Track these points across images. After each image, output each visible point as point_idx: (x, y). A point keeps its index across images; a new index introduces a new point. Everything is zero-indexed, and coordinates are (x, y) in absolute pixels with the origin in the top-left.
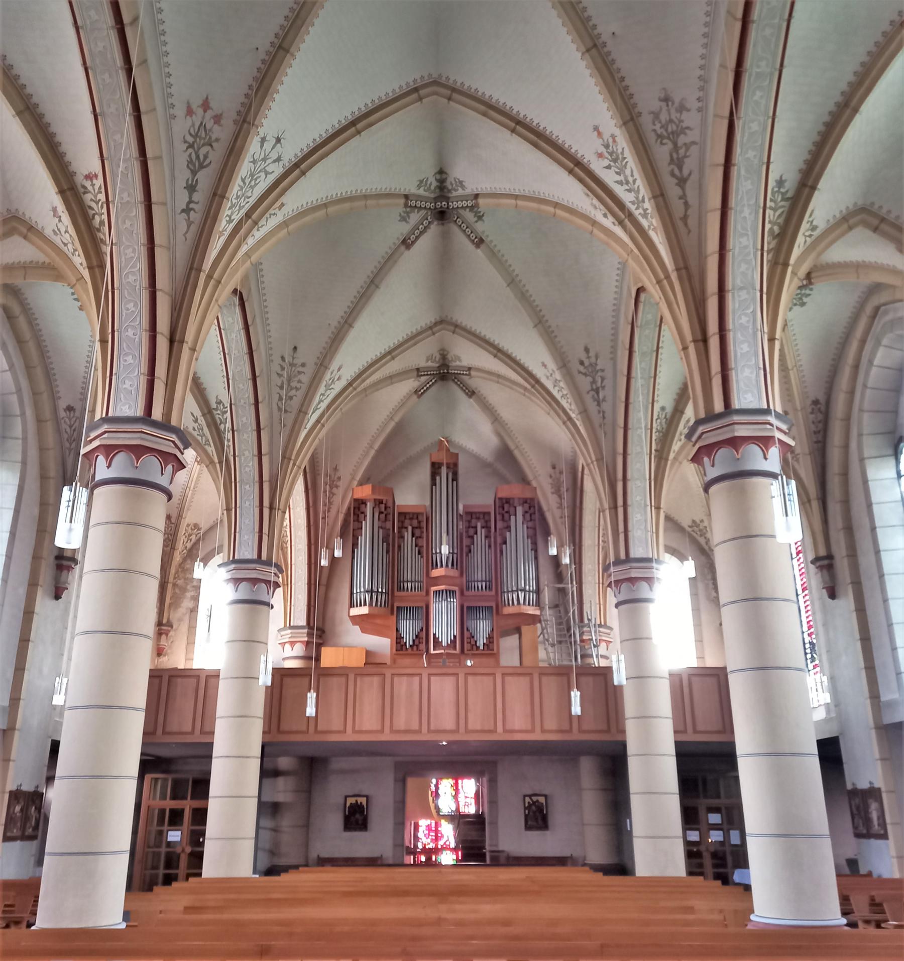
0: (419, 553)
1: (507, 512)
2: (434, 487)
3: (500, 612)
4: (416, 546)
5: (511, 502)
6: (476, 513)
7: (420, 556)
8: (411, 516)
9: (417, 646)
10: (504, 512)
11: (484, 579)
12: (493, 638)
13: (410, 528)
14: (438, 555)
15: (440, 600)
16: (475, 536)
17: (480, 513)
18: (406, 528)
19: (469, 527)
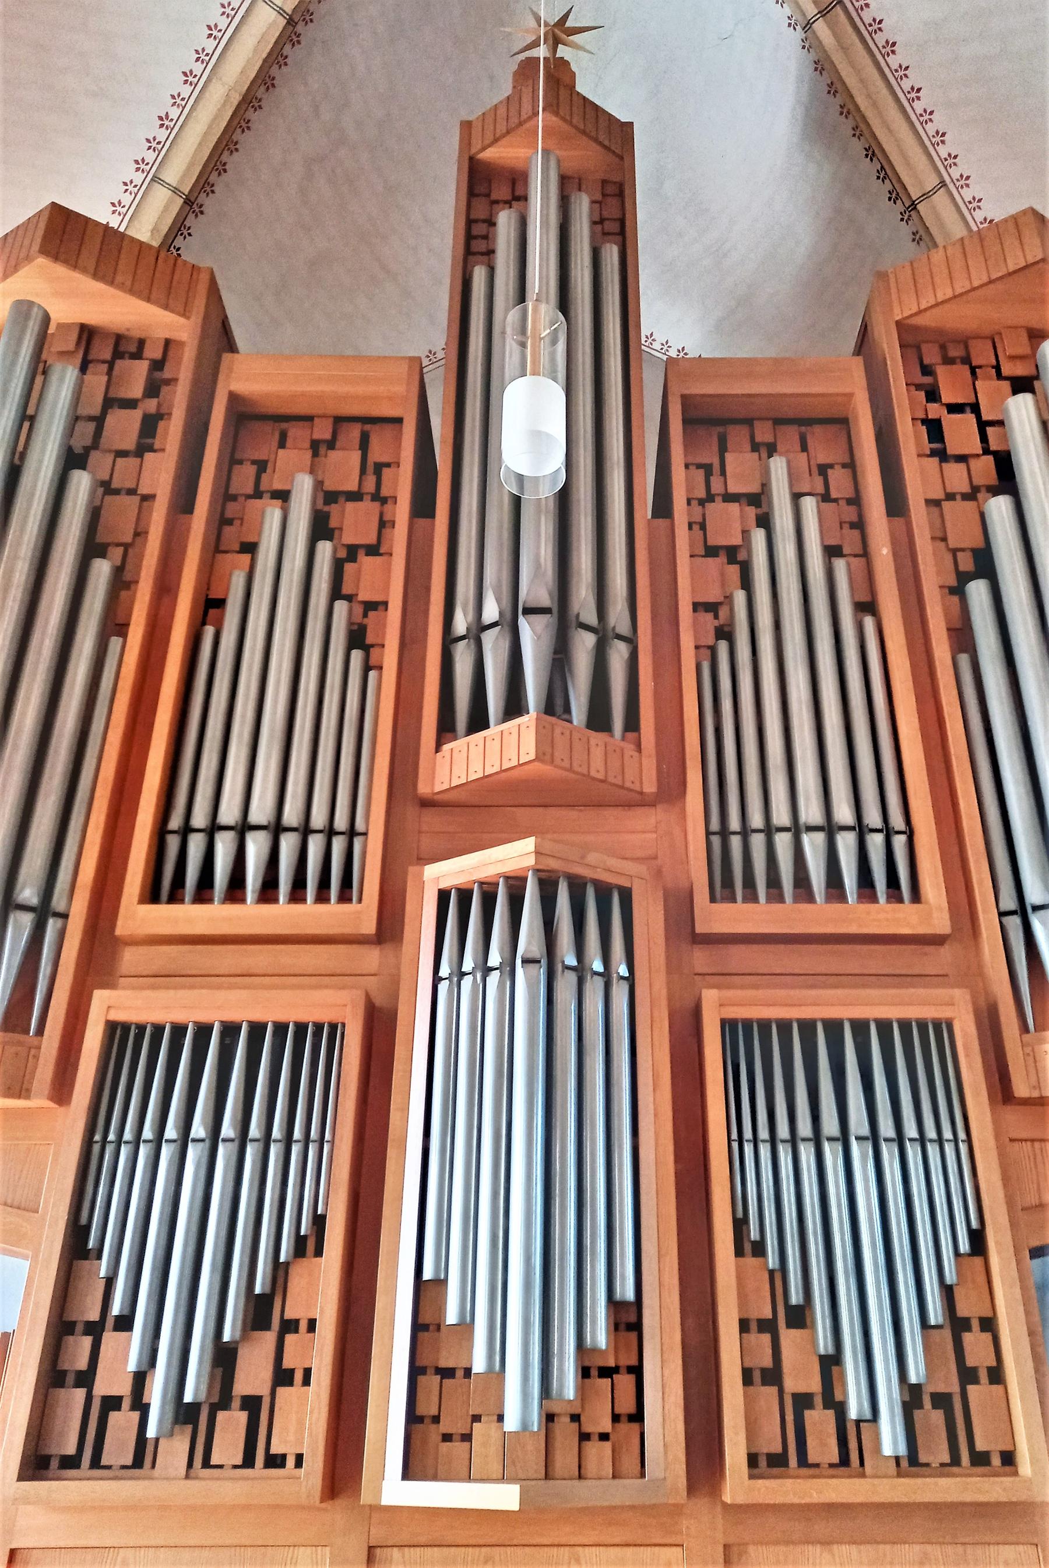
0: (357, 638)
1: (954, 408)
2: (479, 274)
3: (1021, 1089)
4: (336, 593)
5: (982, 355)
6: (748, 422)
7: (357, 656)
8: (323, 431)
9: (251, 1404)
10: (935, 411)
11: (844, 813)
12: (989, 1324)
13: (303, 489)
14: (489, 639)
15: (495, 959)
16: (759, 537)
17: (779, 422)
18: (283, 496)
19: (710, 498)
